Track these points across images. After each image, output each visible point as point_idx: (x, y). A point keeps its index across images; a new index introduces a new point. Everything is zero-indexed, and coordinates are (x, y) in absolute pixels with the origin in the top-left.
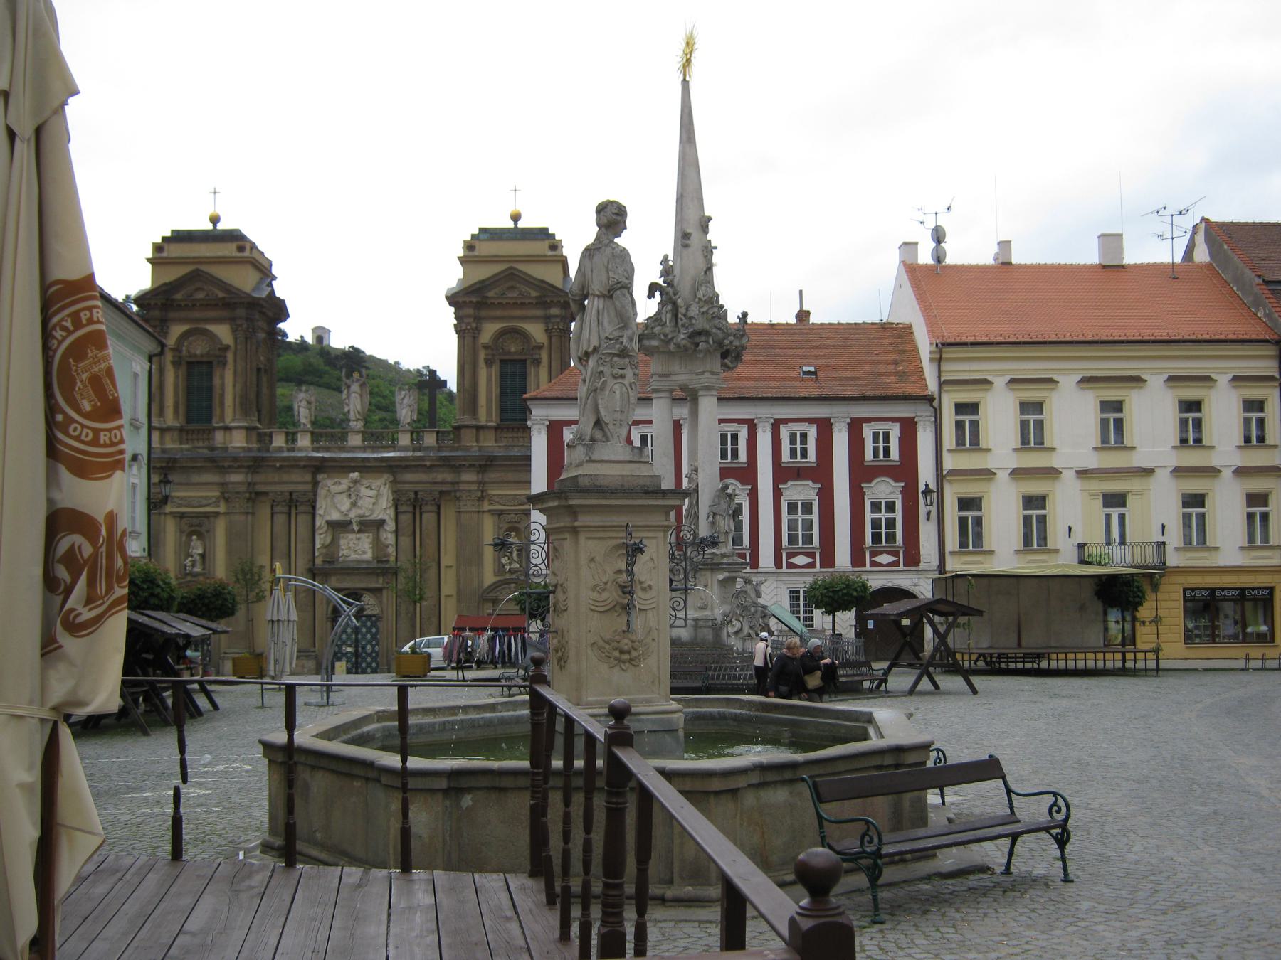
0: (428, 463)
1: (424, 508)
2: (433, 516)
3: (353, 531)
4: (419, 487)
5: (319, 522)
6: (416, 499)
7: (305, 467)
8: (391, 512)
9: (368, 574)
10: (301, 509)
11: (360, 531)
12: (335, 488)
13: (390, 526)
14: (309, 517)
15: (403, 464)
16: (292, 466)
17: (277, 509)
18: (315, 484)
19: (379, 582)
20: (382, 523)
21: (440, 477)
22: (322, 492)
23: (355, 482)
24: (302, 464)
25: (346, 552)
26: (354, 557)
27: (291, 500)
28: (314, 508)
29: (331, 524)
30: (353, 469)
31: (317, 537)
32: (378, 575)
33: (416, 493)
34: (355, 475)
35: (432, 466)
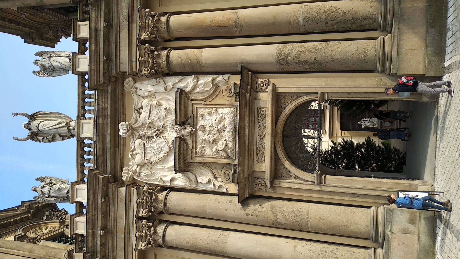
0: (102, 24)
1: (165, 35)
2: (173, 19)
3: (194, 134)
4: (135, 41)
5: (181, 181)
6: (151, 42)
7: (106, 196)
8: (171, 81)
9: (251, 112)
10: (160, 206)
11: (194, 125)
12: (139, 158)
13: (188, 83)
14: (173, 196)
15: (102, 58)
16: (105, 215)
17: (159, 239)
18: (134, 183)
19: (265, 98)
20: (183, 96)
21: (125, 11)
22: (144, 176)
23: (131, 130)
24: (100, 200)
25: (220, 147)
26: (227, 135)
27: (148, 219)
28: (164, 188)
29: (184, 165)
30: (116, 130)
31: (201, 187)
32: (254, 99)
33: (144, 42)
34: (122, 129)
35: (108, 20)
